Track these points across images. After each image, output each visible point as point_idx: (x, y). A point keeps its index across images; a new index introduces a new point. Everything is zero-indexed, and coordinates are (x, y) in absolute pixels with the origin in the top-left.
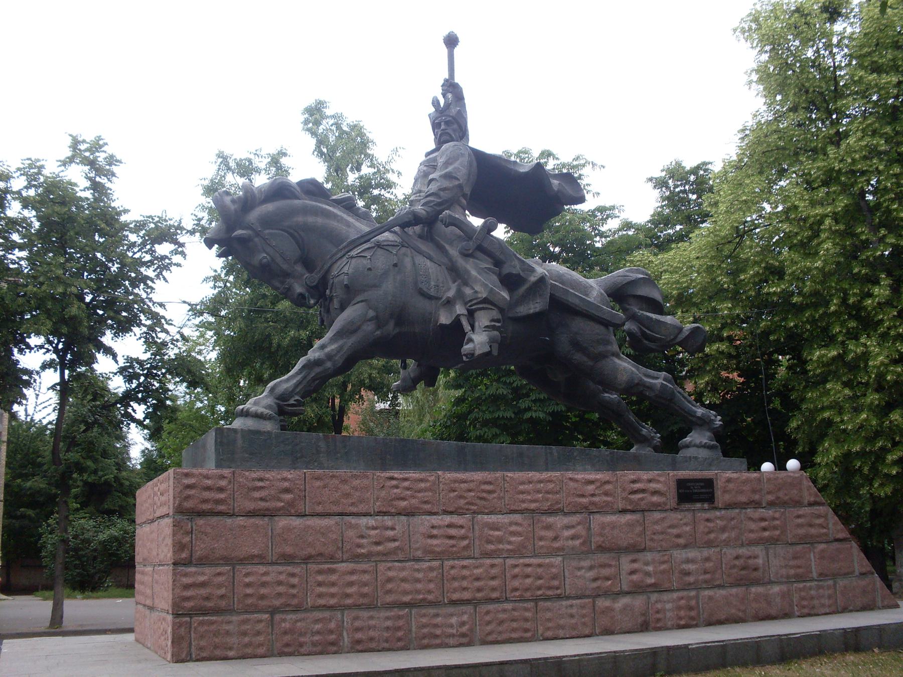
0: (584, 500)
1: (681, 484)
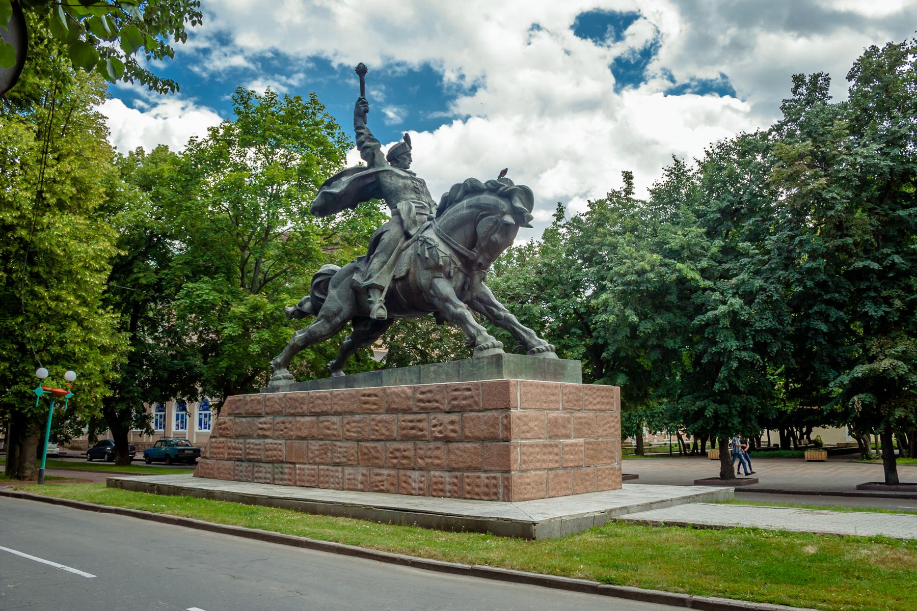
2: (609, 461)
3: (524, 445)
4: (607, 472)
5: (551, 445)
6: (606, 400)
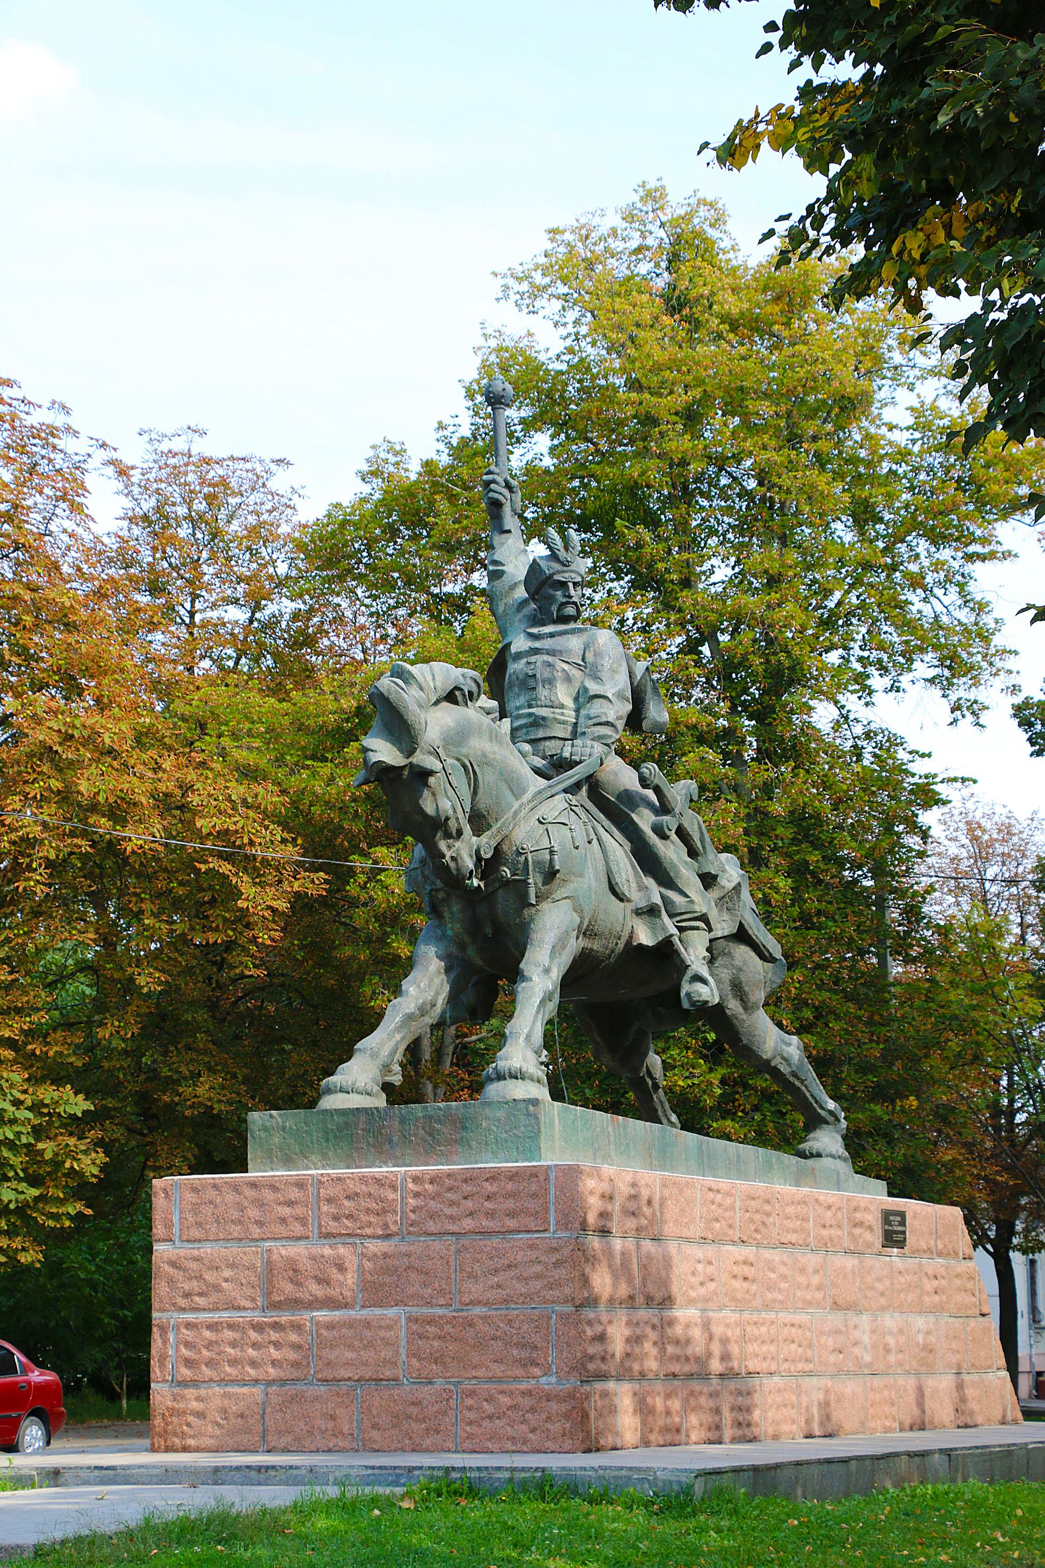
0: (825, 1233)
1: (887, 1216)
2: (519, 1372)
3: (189, 1325)
4: (505, 1400)
5: (276, 1326)
6: (510, 1204)
